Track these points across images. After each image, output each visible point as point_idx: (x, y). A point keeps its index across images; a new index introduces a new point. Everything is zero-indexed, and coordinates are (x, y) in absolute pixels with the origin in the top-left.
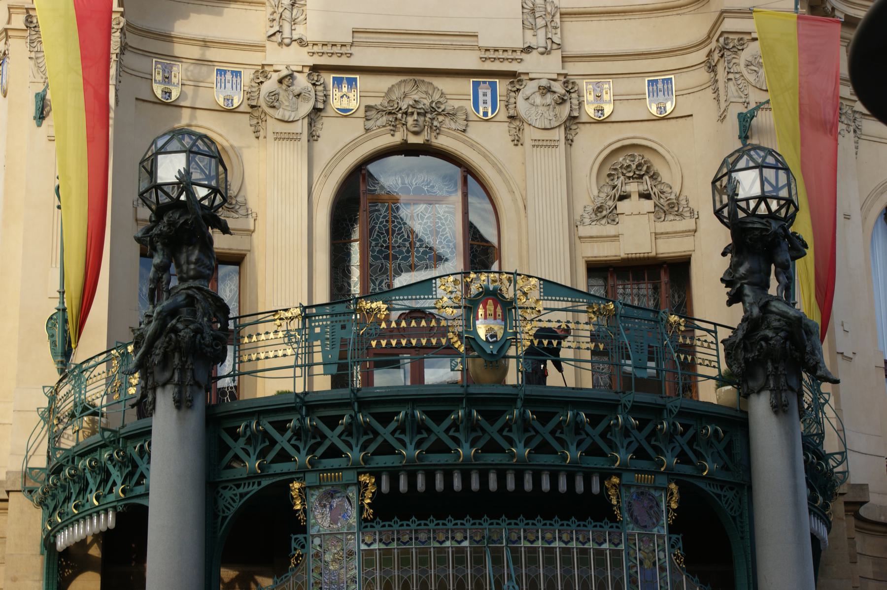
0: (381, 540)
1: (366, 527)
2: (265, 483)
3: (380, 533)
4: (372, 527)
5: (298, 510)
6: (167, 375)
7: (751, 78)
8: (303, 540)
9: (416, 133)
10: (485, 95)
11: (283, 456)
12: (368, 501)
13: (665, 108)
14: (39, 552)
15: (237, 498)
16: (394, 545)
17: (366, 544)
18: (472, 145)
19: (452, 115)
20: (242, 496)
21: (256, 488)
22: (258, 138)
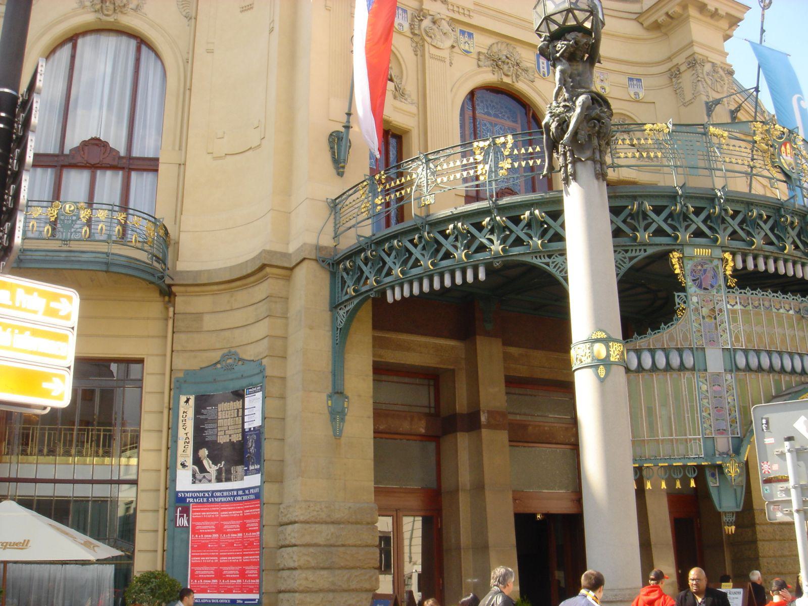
0: (740, 303)
1: (729, 292)
2: (650, 251)
3: (740, 298)
4: (733, 292)
5: (678, 274)
6: (588, 153)
7: (709, 82)
8: (684, 297)
9: (507, 75)
10: (543, 64)
11: (659, 232)
12: (731, 273)
13: (639, 95)
14: (328, 309)
15: (627, 260)
16: (750, 307)
17: (731, 305)
18: (539, 94)
19: (526, 70)
20: (631, 259)
21: (643, 255)
22: (416, 55)
